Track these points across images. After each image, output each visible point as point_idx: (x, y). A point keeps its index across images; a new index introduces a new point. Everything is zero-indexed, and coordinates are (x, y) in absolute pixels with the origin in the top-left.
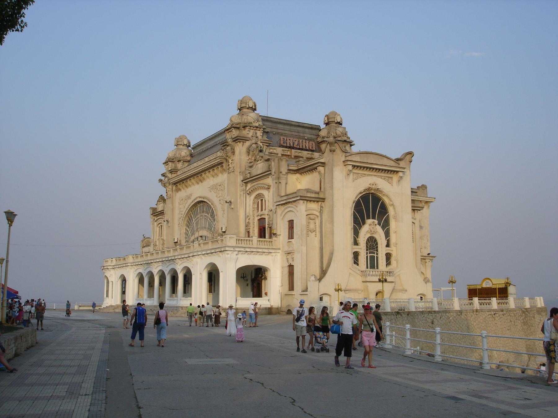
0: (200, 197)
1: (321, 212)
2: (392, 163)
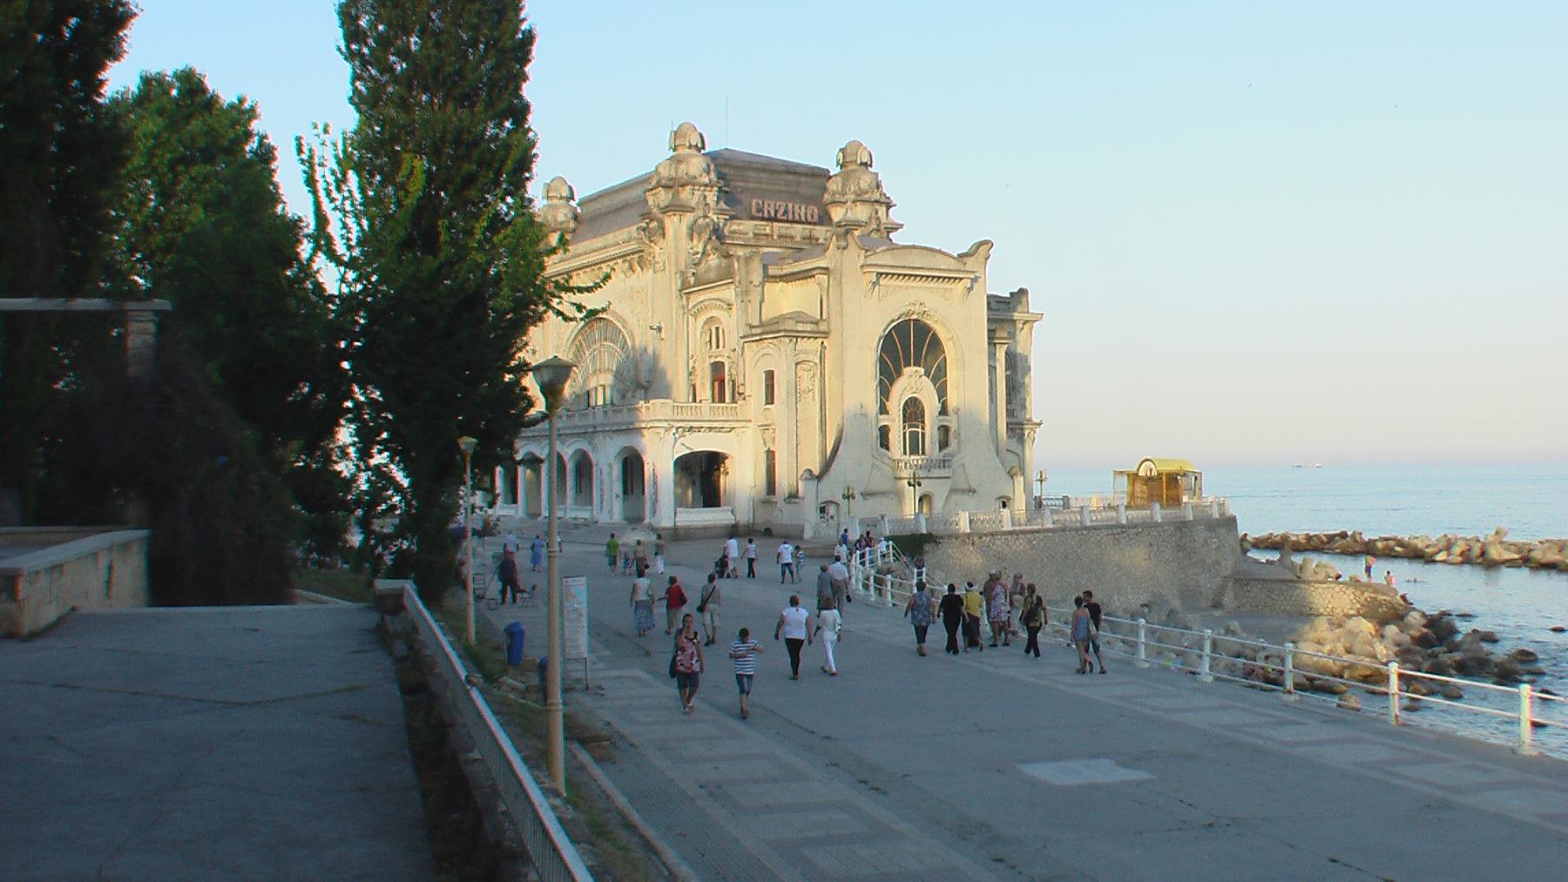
2: (953, 264)
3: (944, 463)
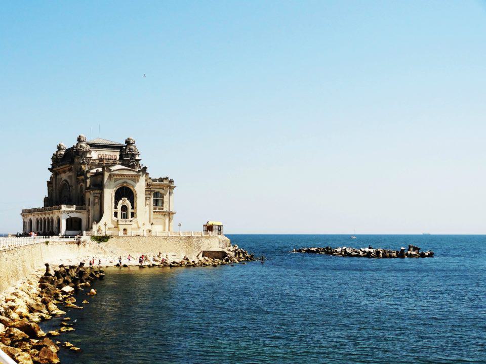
0: (64, 180)
3: (131, 221)
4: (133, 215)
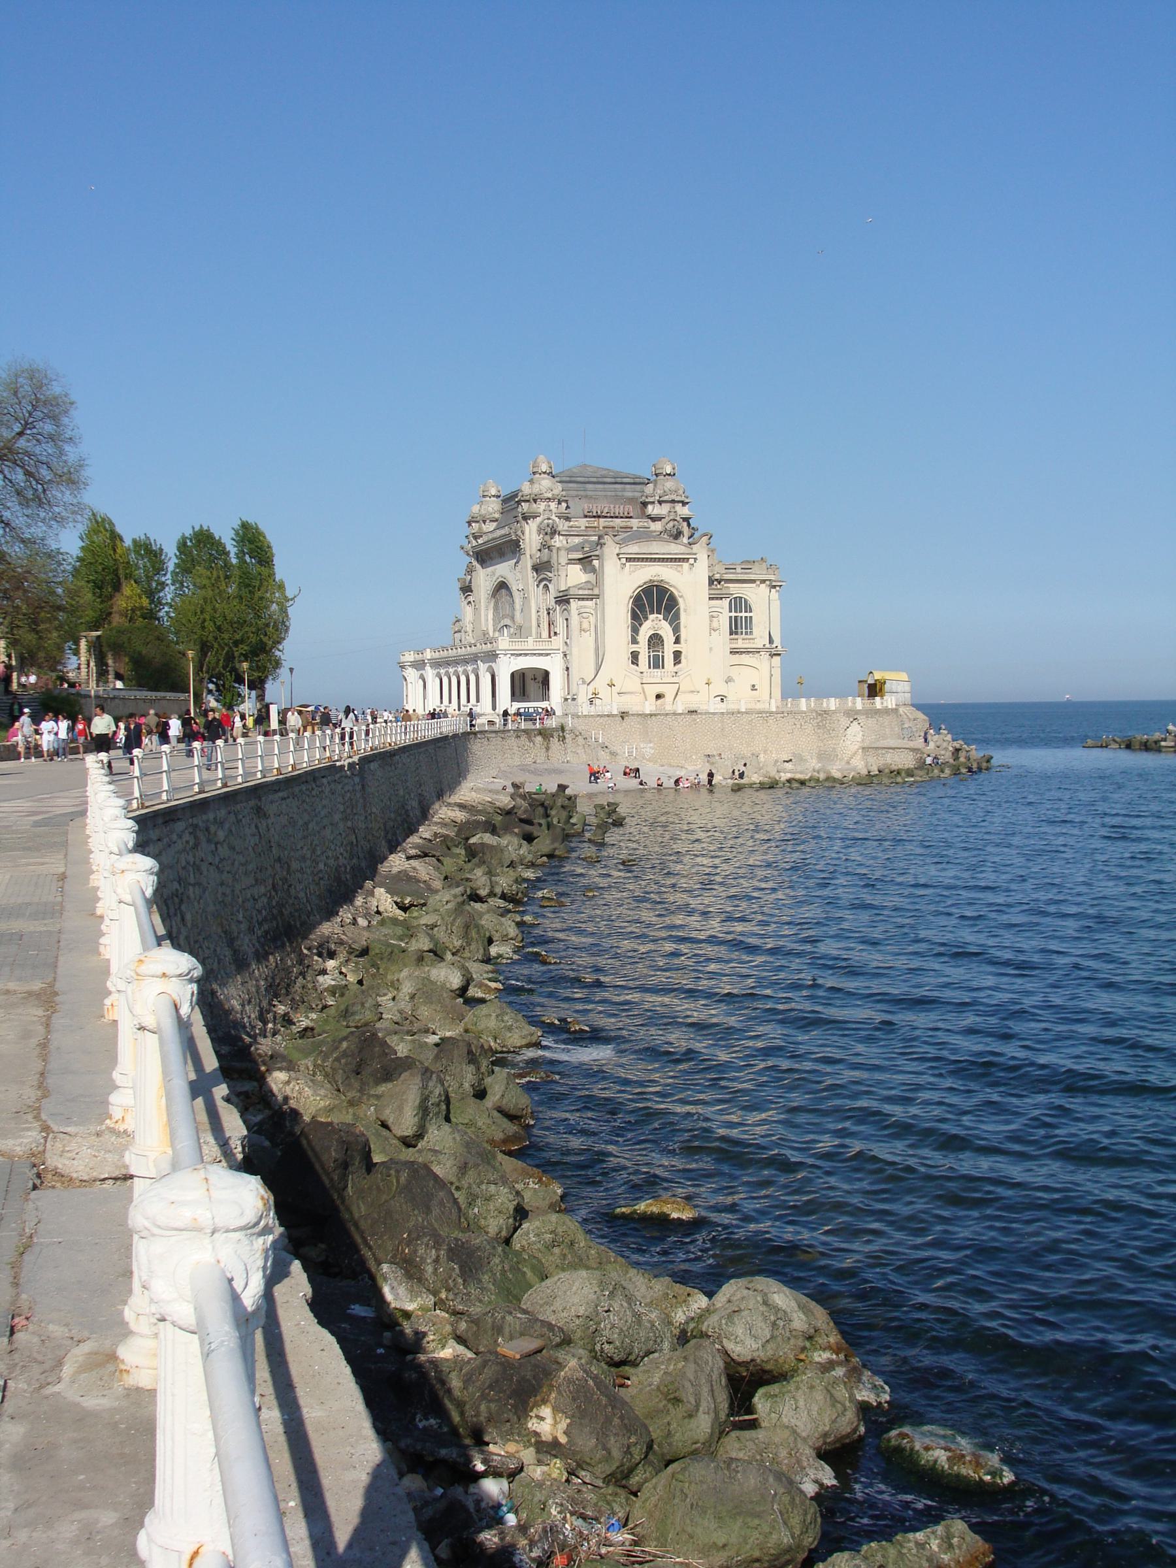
1: (596, 610)
2: (682, 549)
4: (677, 655)
